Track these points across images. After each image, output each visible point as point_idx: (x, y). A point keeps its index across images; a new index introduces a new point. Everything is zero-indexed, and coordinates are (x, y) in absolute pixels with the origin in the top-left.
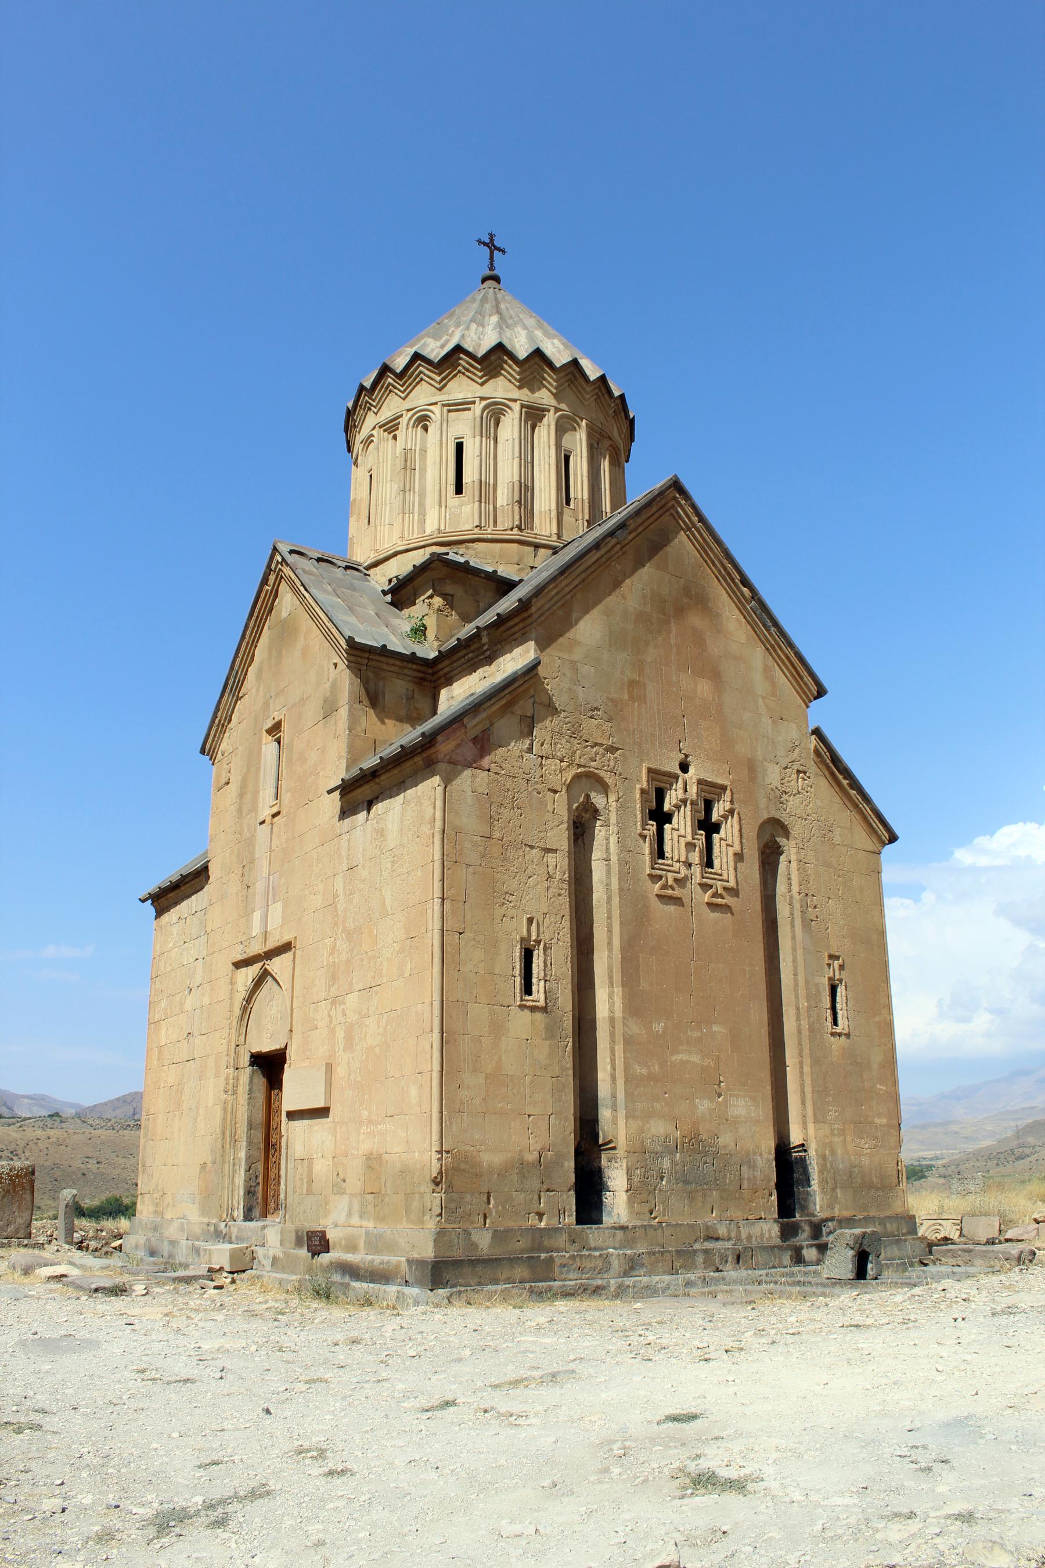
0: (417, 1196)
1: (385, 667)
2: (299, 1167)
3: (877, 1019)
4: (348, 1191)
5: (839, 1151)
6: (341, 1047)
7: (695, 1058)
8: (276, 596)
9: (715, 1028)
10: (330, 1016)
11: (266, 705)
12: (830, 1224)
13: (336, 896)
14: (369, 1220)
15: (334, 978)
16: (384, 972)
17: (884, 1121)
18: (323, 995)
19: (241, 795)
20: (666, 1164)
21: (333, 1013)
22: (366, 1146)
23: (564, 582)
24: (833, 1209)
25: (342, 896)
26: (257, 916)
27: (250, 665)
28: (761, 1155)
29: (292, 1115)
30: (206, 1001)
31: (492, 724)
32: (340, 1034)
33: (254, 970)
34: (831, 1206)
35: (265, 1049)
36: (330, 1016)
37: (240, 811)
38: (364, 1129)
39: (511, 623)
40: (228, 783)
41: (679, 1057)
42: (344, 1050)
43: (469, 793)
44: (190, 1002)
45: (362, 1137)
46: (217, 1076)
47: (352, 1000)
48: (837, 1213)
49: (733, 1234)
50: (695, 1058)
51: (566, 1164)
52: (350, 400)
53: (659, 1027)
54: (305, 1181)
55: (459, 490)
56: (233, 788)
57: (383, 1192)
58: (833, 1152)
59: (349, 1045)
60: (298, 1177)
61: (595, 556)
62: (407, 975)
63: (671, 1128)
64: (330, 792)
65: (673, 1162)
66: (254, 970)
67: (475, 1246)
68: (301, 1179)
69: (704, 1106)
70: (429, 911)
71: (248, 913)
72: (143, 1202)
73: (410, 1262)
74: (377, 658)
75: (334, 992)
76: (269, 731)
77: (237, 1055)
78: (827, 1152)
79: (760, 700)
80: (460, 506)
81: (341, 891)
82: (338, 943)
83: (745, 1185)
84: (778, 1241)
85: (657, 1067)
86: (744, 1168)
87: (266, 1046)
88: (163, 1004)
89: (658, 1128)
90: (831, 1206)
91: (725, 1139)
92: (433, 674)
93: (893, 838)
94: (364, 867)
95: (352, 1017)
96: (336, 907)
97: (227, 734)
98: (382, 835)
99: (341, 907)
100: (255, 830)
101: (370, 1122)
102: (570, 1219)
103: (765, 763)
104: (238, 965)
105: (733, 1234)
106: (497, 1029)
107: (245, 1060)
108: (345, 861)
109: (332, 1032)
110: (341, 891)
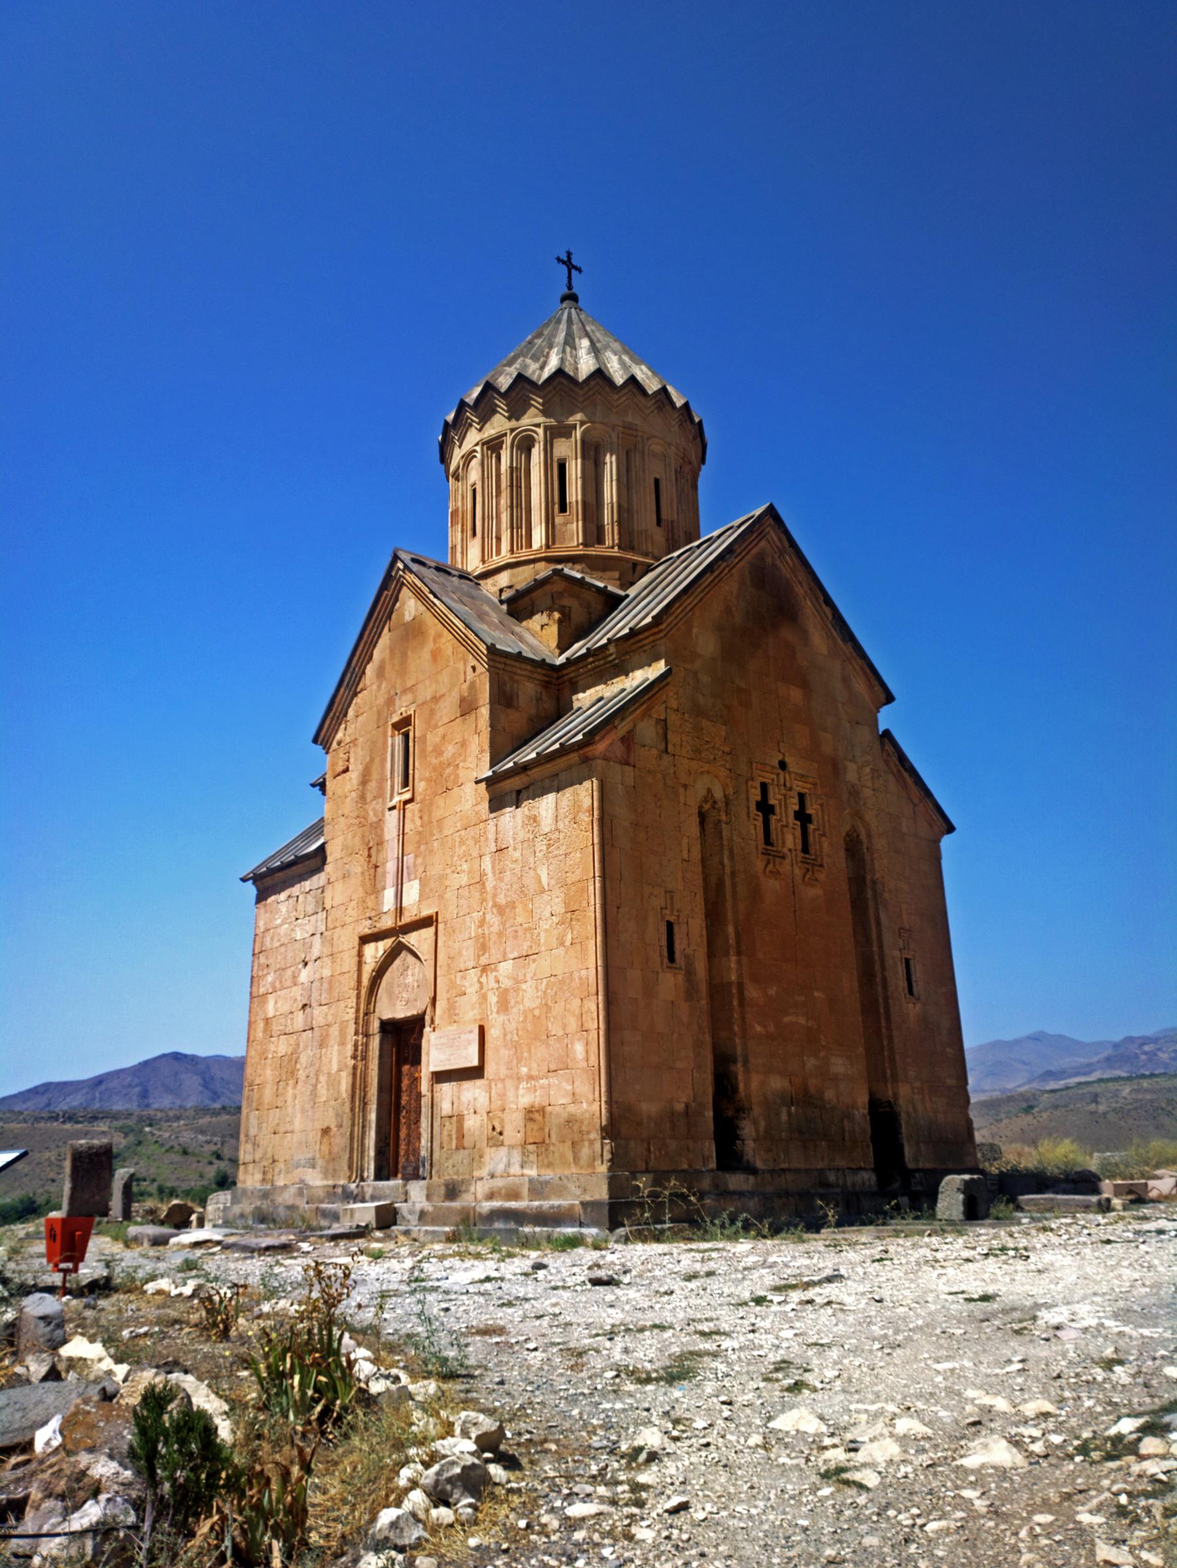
0: (586, 1143)
1: (519, 671)
2: (447, 1124)
4: (506, 1143)
5: (920, 1107)
6: (495, 1010)
7: (802, 1020)
8: (397, 600)
9: (816, 994)
10: (480, 983)
11: (390, 702)
13: (483, 874)
14: (531, 1168)
15: (484, 948)
16: (542, 941)
18: (471, 964)
19: (364, 782)
20: (784, 1117)
21: (483, 980)
22: (526, 1099)
25: (490, 875)
26: (389, 895)
27: (368, 663)
29: (440, 1077)
30: (327, 972)
31: (635, 726)
32: (493, 999)
33: (383, 946)
35: (400, 1015)
36: (480, 983)
37: (362, 798)
38: (523, 1085)
39: (641, 637)
40: (346, 770)
41: (787, 1019)
42: (498, 1012)
44: (305, 975)
45: (521, 1092)
46: (342, 1043)
47: (506, 967)
50: (802, 1020)
51: (707, 1114)
52: (448, 413)
53: (772, 991)
54: (454, 1136)
55: (563, 509)
56: (354, 776)
57: (547, 1141)
59: (504, 1006)
60: (445, 1133)
61: (709, 578)
62: (568, 943)
63: (786, 1084)
64: (477, 782)
65: (789, 1114)
66: (383, 946)
68: (450, 1136)
70: (591, 888)
71: (374, 889)
72: (246, 1172)
73: (582, 1203)
74: (513, 663)
75: (484, 960)
76: (397, 726)
77: (367, 1024)
79: (840, 705)
80: (566, 524)
81: (489, 870)
82: (488, 917)
86: (846, 1122)
87: (401, 1012)
88: (270, 978)
89: (777, 1083)
90: (916, 1160)
92: (558, 678)
93: (951, 829)
94: (515, 849)
95: (506, 983)
96: (484, 884)
97: (343, 726)
98: (535, 821)
99: (490, 883)
100: (383, 815)
101: (530, 1078)
102: (713, 1165)
104: (364, 940)
105: (841, 1182)
106: (649, 991)
107: (375, 1026)
108: (493, 844)
109: (484, 997)
110: (489, 870)
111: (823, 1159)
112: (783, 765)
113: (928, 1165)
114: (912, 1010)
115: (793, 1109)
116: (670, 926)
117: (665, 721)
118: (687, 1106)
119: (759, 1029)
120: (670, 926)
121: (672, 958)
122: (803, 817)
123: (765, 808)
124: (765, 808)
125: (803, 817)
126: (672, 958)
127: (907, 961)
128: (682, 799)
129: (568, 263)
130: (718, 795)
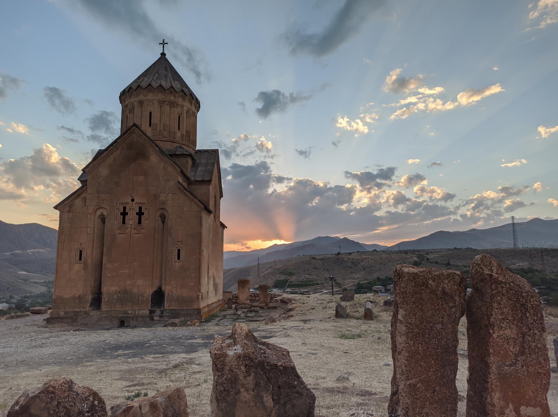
3: (194, 257)
5: (175, 292)
9: (134, 264)
12: (167, 311)
17: (193, 284)
20: (115, 296)
23: (95, 162)
24: (170, 307)
28: (146, 294)
34: (170, 306)
43: (67, 218)
48: (171, 308)
49: (133, 313)
50: (127, 271)
53: (116, 265)
58: (172, 292)
65: (117, 296)
67: (60, 315)
69: (128, 282)
78: (170, 293)
79: (161, 177)
83: (140, 301)
84: (148, 315)
85: (115, 274)
86: (140, 297)
89: (114, 288)
90: (170, 306)
91: (135, 290)
103: (160, 194)
105: (133, 313)
111: (129, 307)
112: (133, 200)
113: (174, 308)
114: (178, 265)
115: (119, 295)
116: (81, 252)
117: (86, 197)
118: (80, 295)
119: (109, 275)
120: (81, 252)
121: (80, 259)
122: (140, 214)
123: (124, 214)
124: (124, 214)
125: (140, 214)
126: (80, 259)
127: (179, 251)
128: (89, 218)
129: (164, 44)
130: (105, 213)
